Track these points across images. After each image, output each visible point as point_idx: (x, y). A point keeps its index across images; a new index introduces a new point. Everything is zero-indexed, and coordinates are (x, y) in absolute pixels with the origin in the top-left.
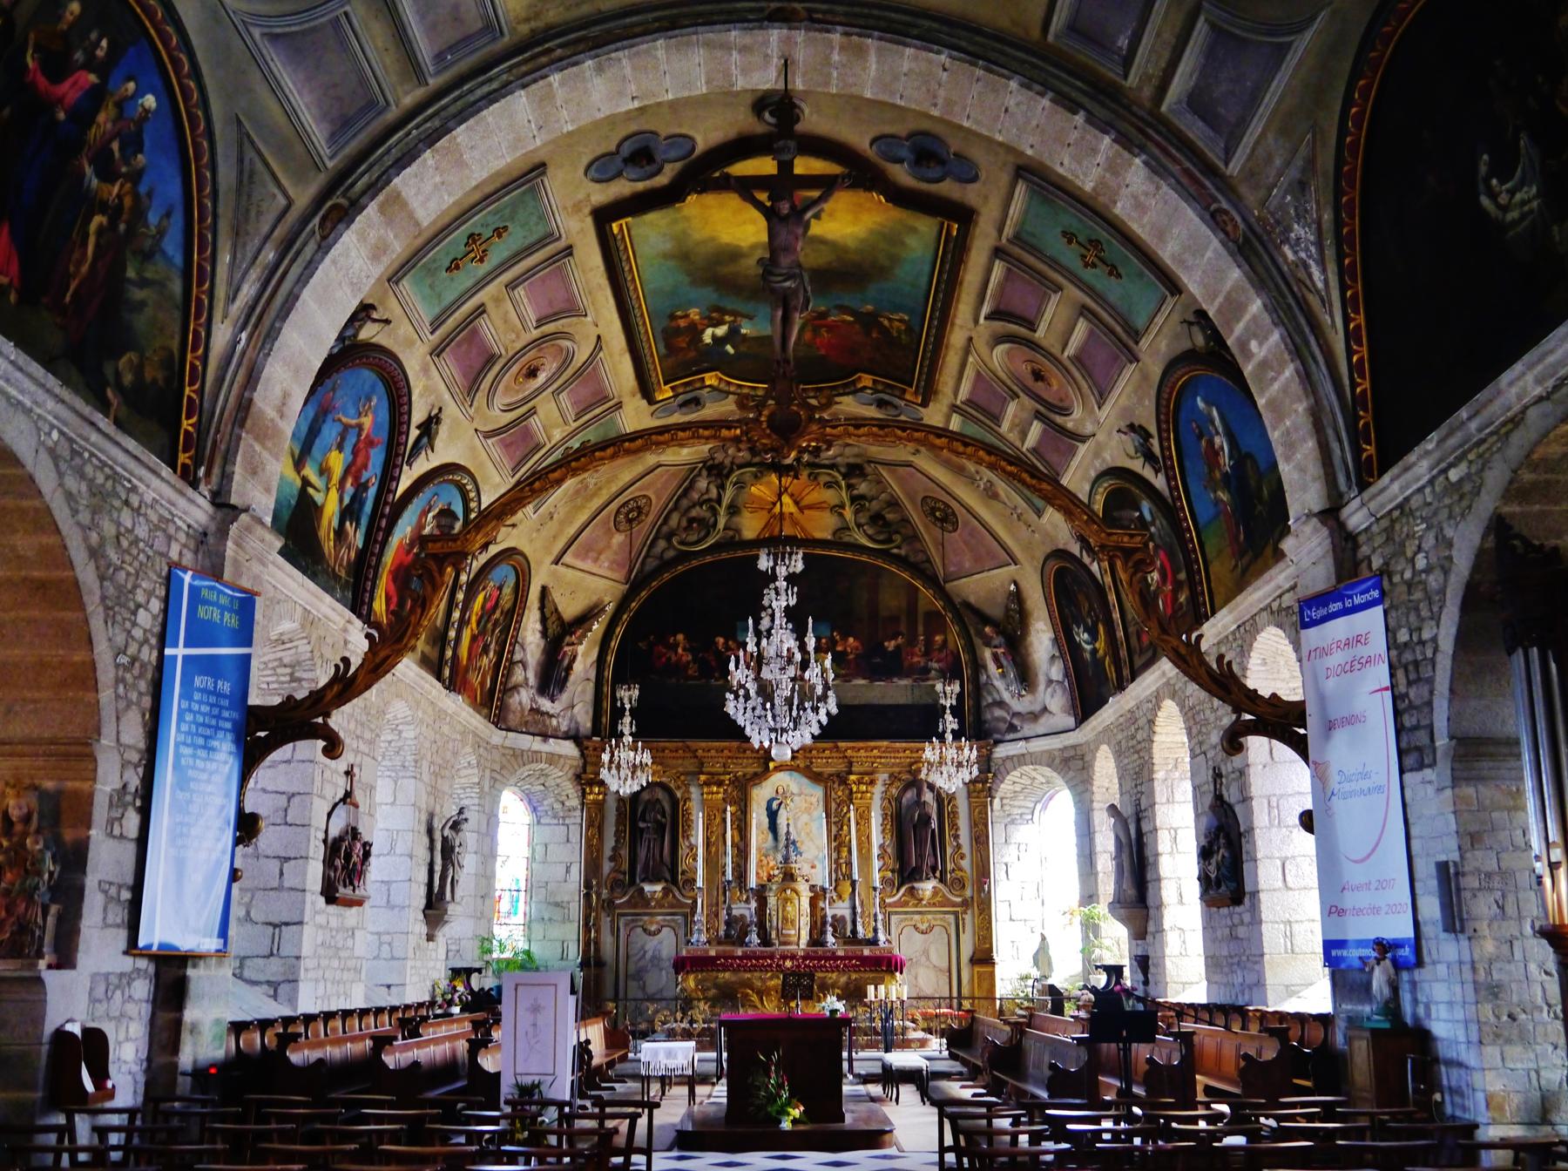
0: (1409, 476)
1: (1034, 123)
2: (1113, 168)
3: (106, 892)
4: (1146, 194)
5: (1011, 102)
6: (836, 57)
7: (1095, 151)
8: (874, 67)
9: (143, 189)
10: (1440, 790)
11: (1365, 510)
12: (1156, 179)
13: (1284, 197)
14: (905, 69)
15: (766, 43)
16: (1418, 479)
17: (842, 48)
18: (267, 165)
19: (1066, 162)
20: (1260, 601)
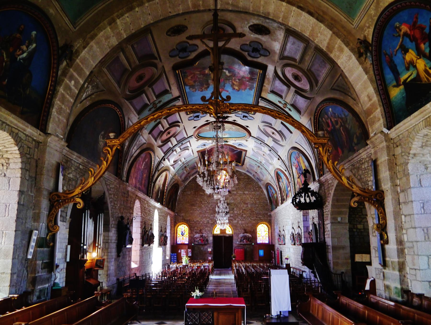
0: (78, 159)
1: (141, 19)
2: (119, 34)
3: (375, 249)
4: (109, 42)
5: (150, 17)
6: (201, 2)
7: (125, 31)
8: (189, 3)
9: (340, 116)
10: (66, 228)
11: (66, 152)
12: (111, 48)
13: (96, 82)
14: (181, 6)
15: (221, 5)
16: (78, 161)
17: (199, 6)
18: (336, 81)
19: (128, 19)
20: (11, 122)
